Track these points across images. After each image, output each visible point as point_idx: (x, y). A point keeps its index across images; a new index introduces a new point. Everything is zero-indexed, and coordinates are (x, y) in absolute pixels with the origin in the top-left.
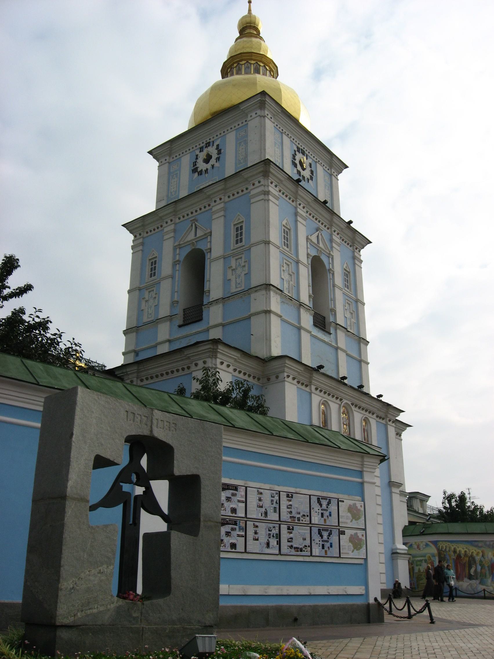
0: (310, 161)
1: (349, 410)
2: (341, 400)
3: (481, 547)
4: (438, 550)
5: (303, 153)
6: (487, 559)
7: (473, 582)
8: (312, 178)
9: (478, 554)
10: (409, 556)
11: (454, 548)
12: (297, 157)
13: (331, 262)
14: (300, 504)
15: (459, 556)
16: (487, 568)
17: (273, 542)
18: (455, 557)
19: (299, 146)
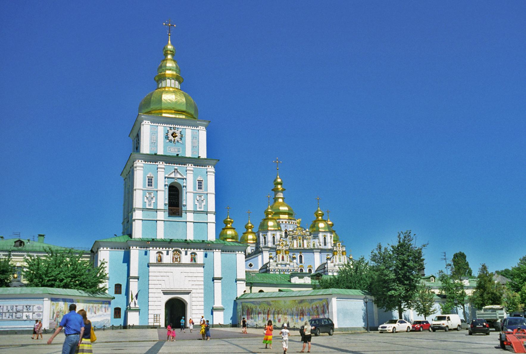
5: (174, 128)
7: (253, 320)
8: (181, 139)
14: (20, 308)
15: (248, 309)
17: (11, 317)
18: (247, 309)
19: (172, 126)
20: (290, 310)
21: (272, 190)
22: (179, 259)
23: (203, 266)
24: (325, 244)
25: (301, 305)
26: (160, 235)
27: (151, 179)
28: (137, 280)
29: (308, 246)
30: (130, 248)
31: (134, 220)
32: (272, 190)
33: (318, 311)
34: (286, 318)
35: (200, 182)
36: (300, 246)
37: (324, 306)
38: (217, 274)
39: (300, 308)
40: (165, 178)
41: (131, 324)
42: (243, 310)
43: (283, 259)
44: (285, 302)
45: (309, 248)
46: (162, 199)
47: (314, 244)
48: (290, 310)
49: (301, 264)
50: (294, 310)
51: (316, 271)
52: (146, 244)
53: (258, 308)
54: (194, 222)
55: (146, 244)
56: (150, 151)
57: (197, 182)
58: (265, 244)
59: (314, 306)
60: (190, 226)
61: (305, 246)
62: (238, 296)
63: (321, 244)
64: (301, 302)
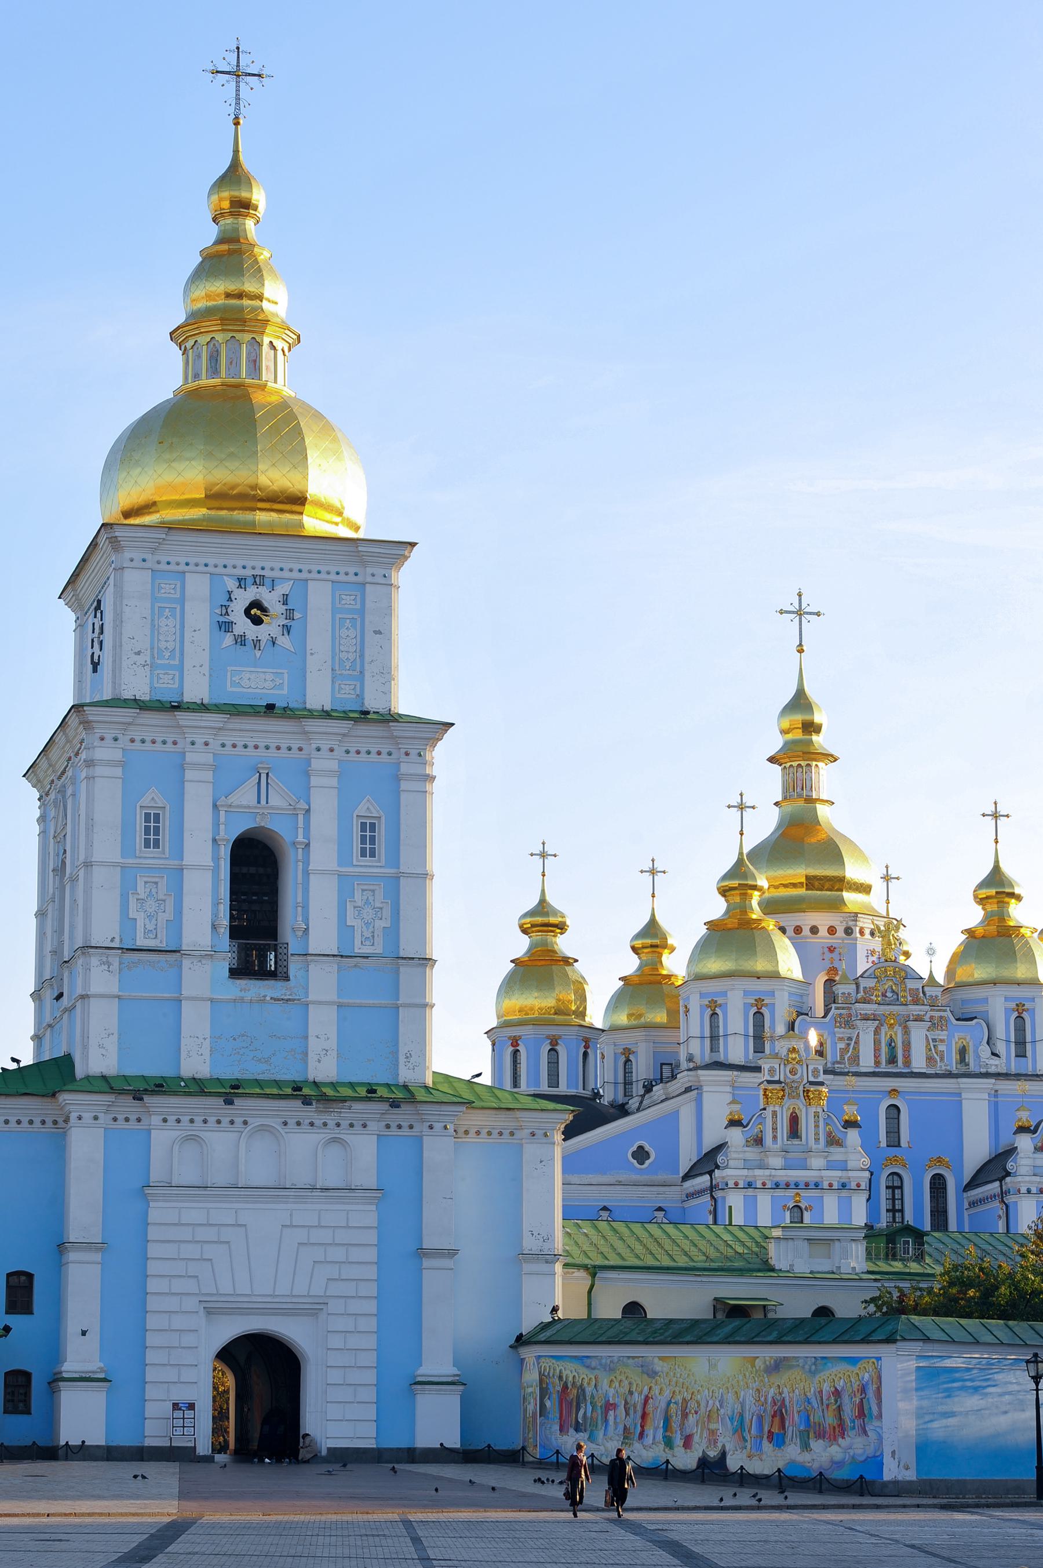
0: (283, 588)
3: (594, 1369)
4: (540, 1373)
5: (258, 580)
6: (600, 1391)
7: (582, 1437)
9: (589, 1384)
10: (461, 1388)
11: (561, 1372)
12: (233, 606)
13: (301, 824)
15: (565, 1387)
16: (599, 1411)
18: (559, 1388)
19: (249, 572)
20: (730, 1398)
21: (772, 760)
24: (1021, 1054)
25: (777, 1380)
26: (196, 1063)
27: (157, 817)
28: (98, 1257)
29: (930, 1059)
30: (67, 1120)
32: (772, 760)
33: (839, 1409)
34: (713, 1432)
35: (368, 829)
36: (892, 1060)
37: (863, 1390)
39: (772, 1392)
41: (75, 1442)
42: (544, 1392)
43: (794, 1131)
44: (712, 1366)
45: (940, 1067)
47: (963, 1052)
48: (730, 1398)
49: (894, 1151)
50: (750, 1401)
51: (974, 1183)
53: (605, 1383)
54: (340, 1006)
56: (152, 688)
58: (714, 1049)
59: (826, 1388)
60: (323, 1027)
61: (919, 1063)
62: (527, 1327)
63: (1001, 1048)
64: (777, 1366)
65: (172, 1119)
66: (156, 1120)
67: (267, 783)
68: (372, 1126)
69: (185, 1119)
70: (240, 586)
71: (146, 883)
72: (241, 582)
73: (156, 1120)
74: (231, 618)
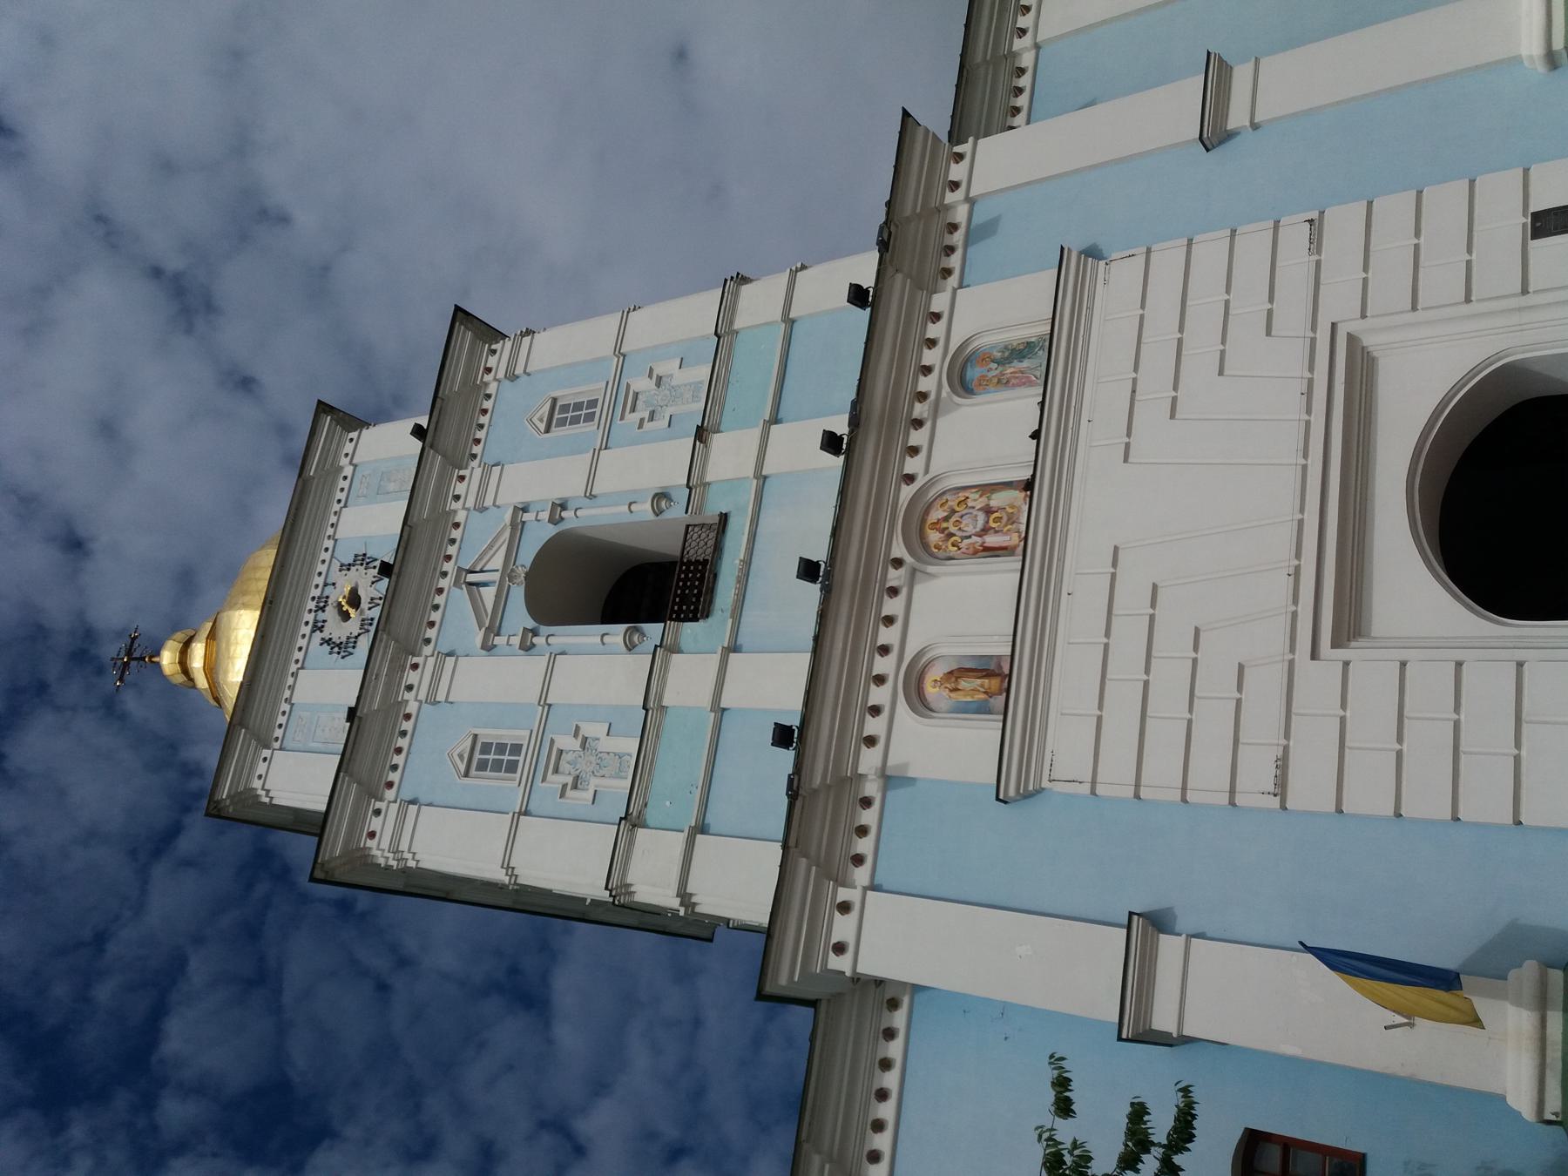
1: (932, 493)
2: (898, 563)
22: (998, 499)
23: (1077, 266)
27: (486, 748)
28: (1170, 947)
31: (684, 896)
38: (1177, 108)
40: (488, 647)
46: (599, 667)
52: (821, 812)
55: (821, 812)
57: (557, 432)
65: (874, 726)
66: (869, 760)
67: (482, 571)
68: (939, 303)
69: (878, 695)
70: (321, 629)
71: (556, 771)
72: (318, 627)
73: (869, 760)
74: (344, 639)
